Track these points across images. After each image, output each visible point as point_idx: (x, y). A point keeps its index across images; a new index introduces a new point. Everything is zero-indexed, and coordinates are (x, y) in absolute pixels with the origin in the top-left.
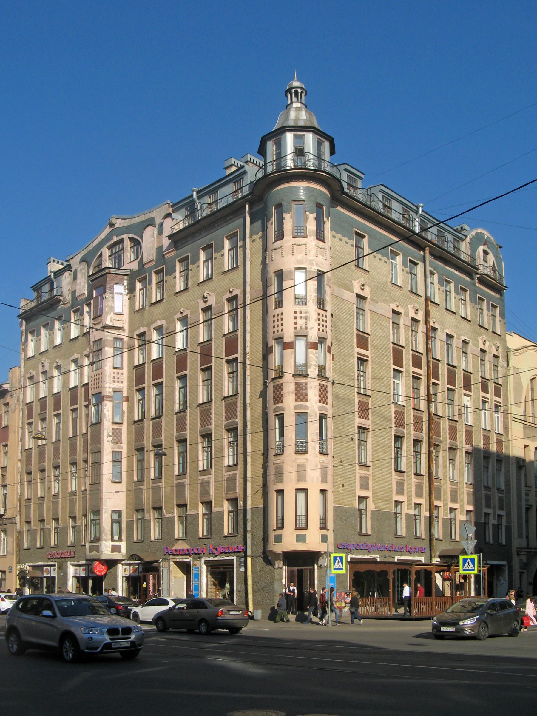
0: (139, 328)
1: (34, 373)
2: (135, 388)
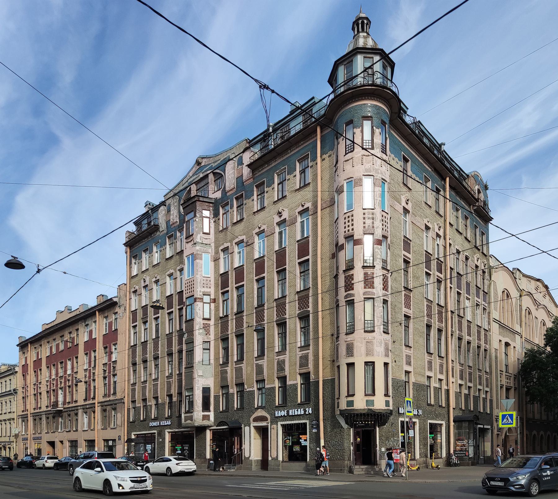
0: (223, 244)
1: (137, 287)
2: (221, 291)
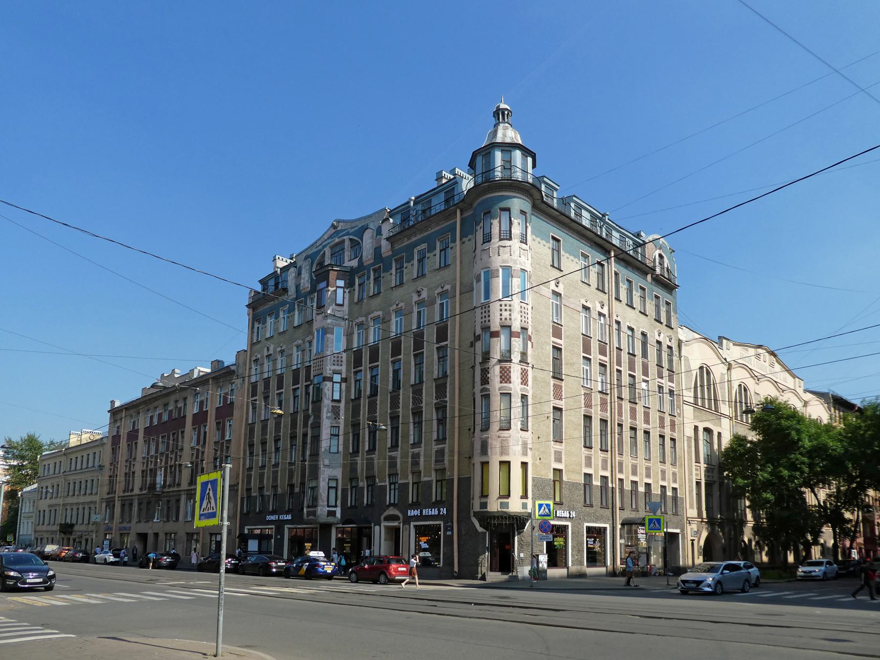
1: (259, 356)
2: (353, 370)
